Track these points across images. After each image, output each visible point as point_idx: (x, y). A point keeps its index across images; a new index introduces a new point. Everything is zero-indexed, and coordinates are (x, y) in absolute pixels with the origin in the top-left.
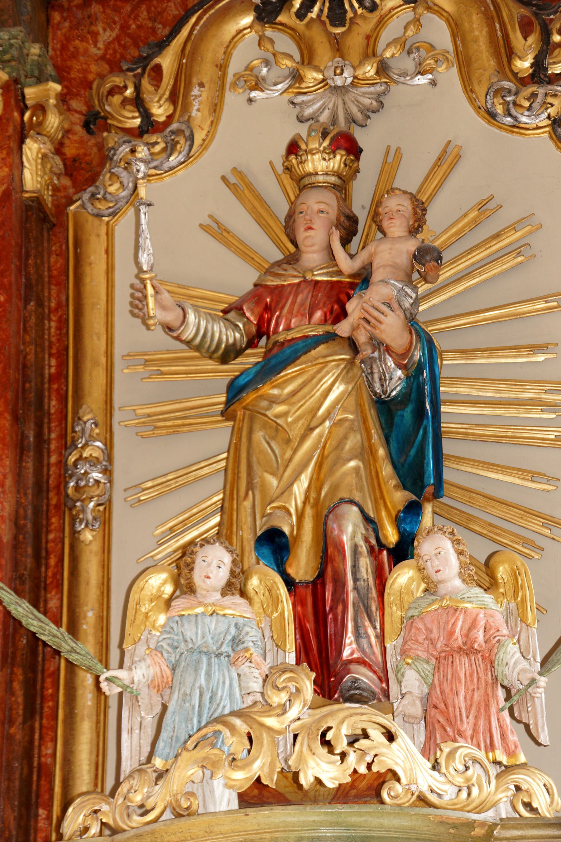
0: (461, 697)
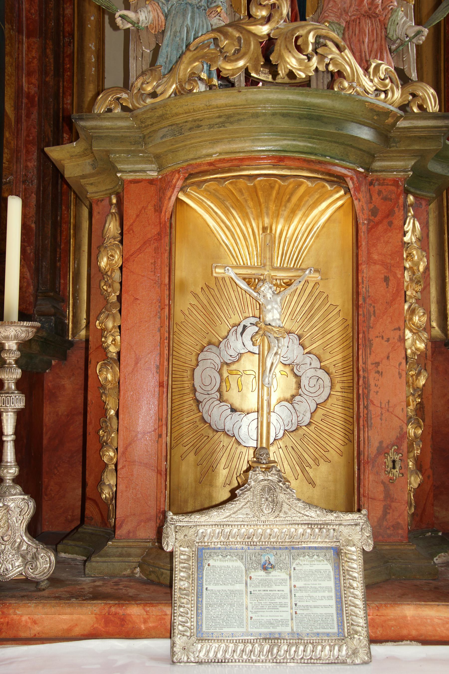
0: (366, 45)
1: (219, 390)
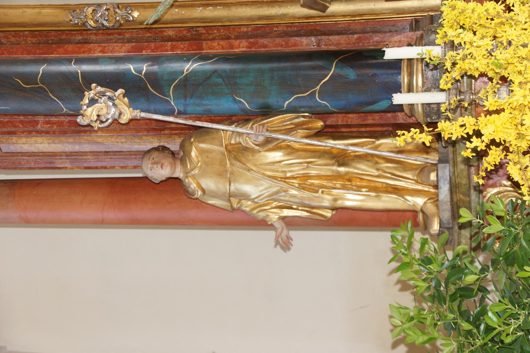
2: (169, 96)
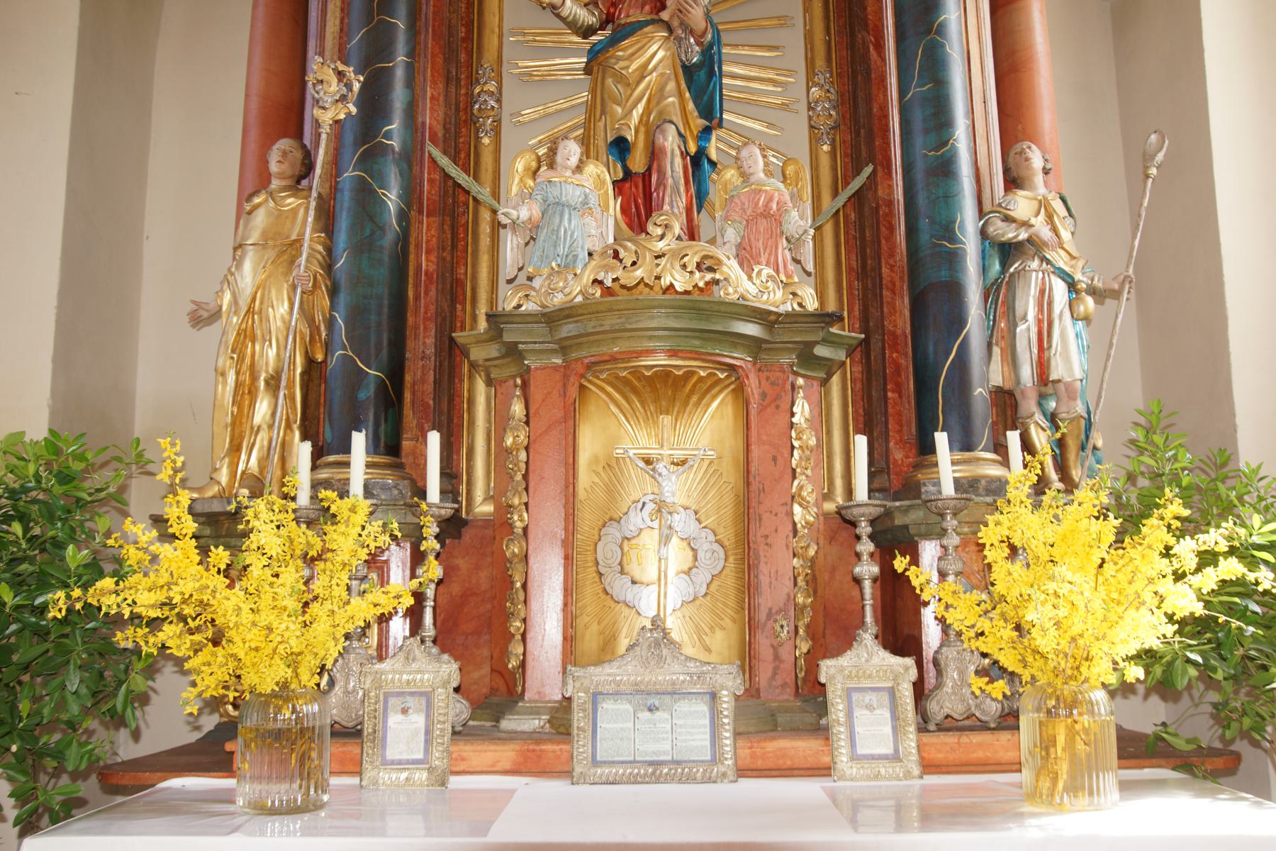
1: (621, 564)
2: (353, 171)
